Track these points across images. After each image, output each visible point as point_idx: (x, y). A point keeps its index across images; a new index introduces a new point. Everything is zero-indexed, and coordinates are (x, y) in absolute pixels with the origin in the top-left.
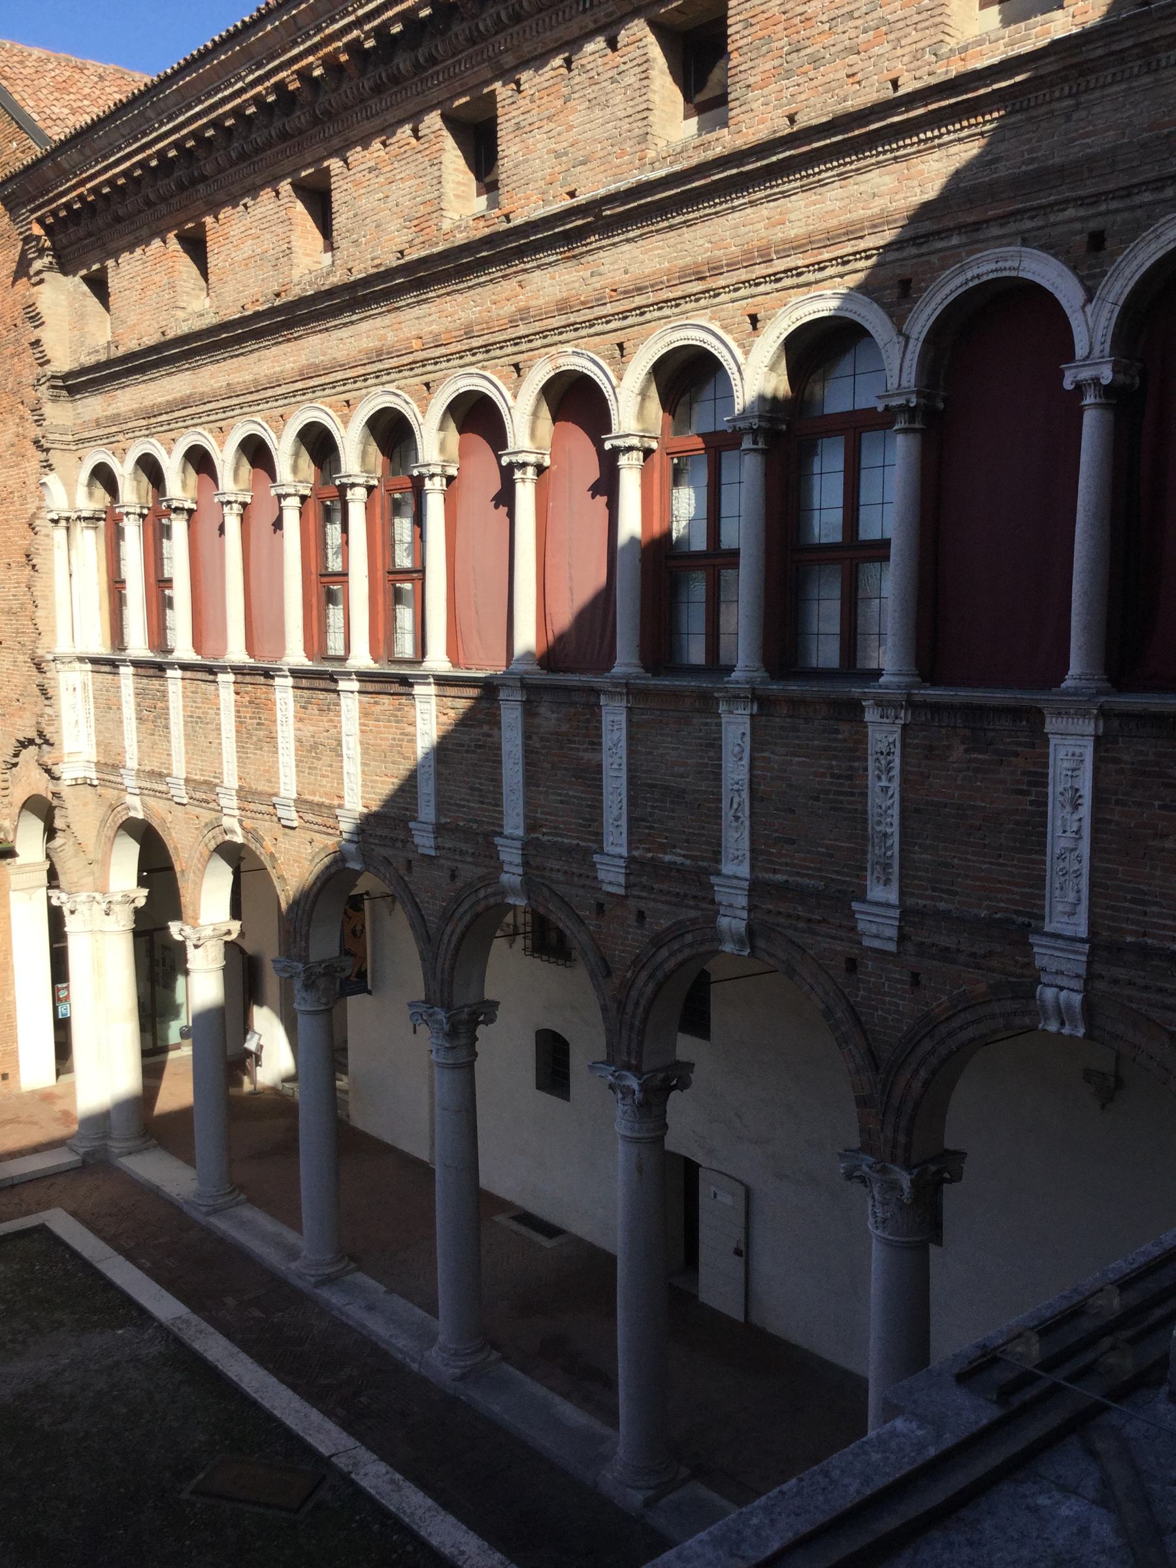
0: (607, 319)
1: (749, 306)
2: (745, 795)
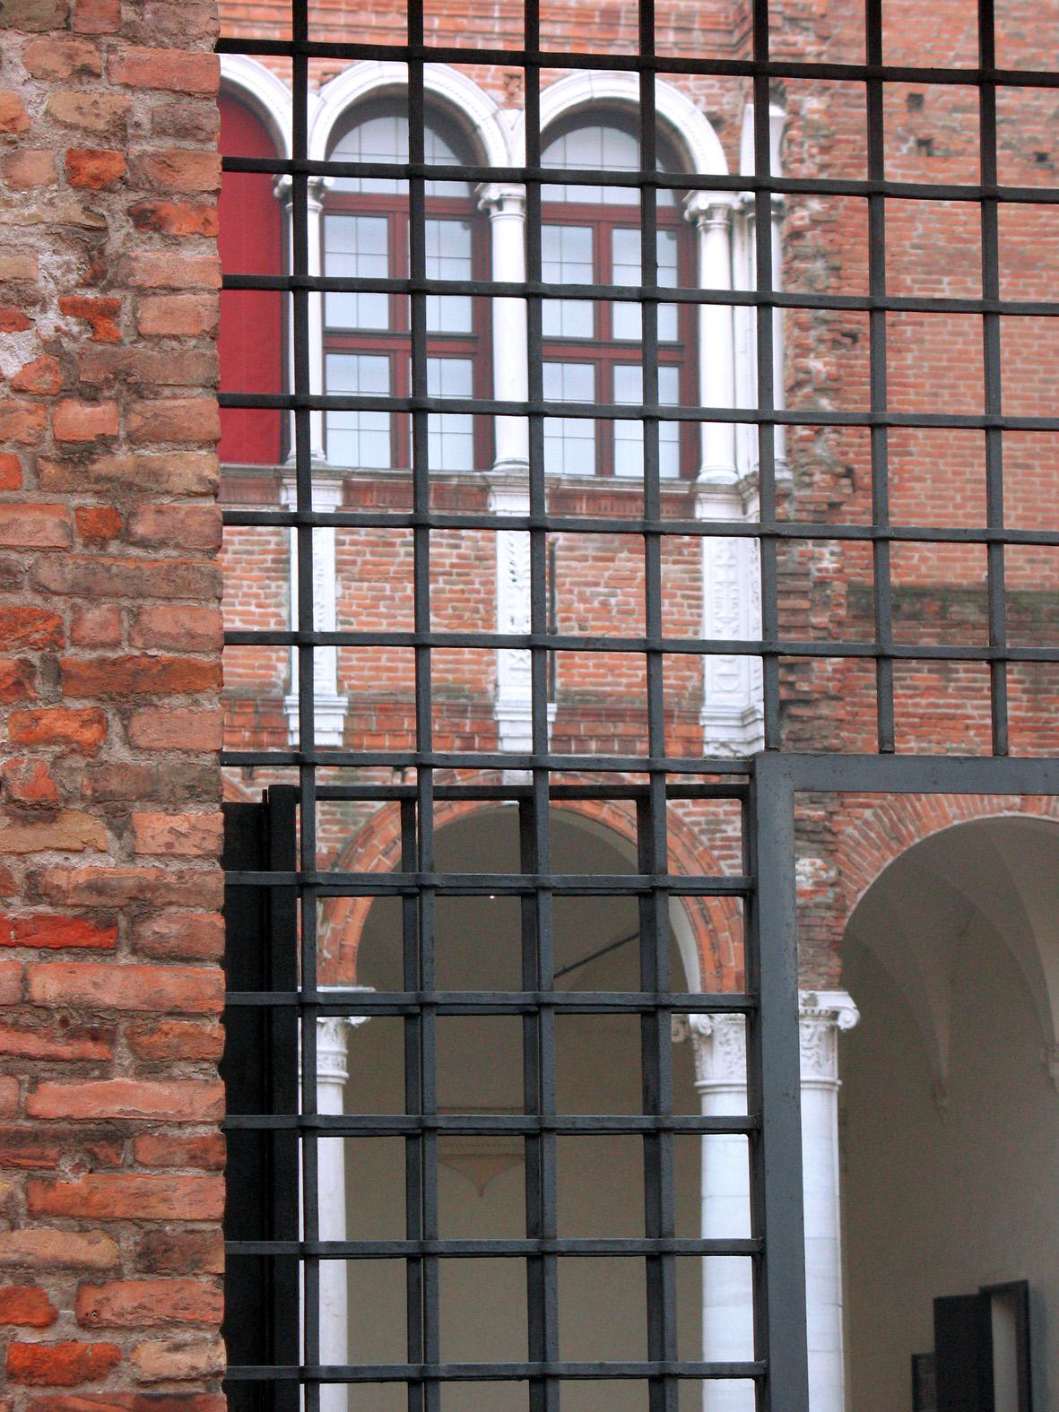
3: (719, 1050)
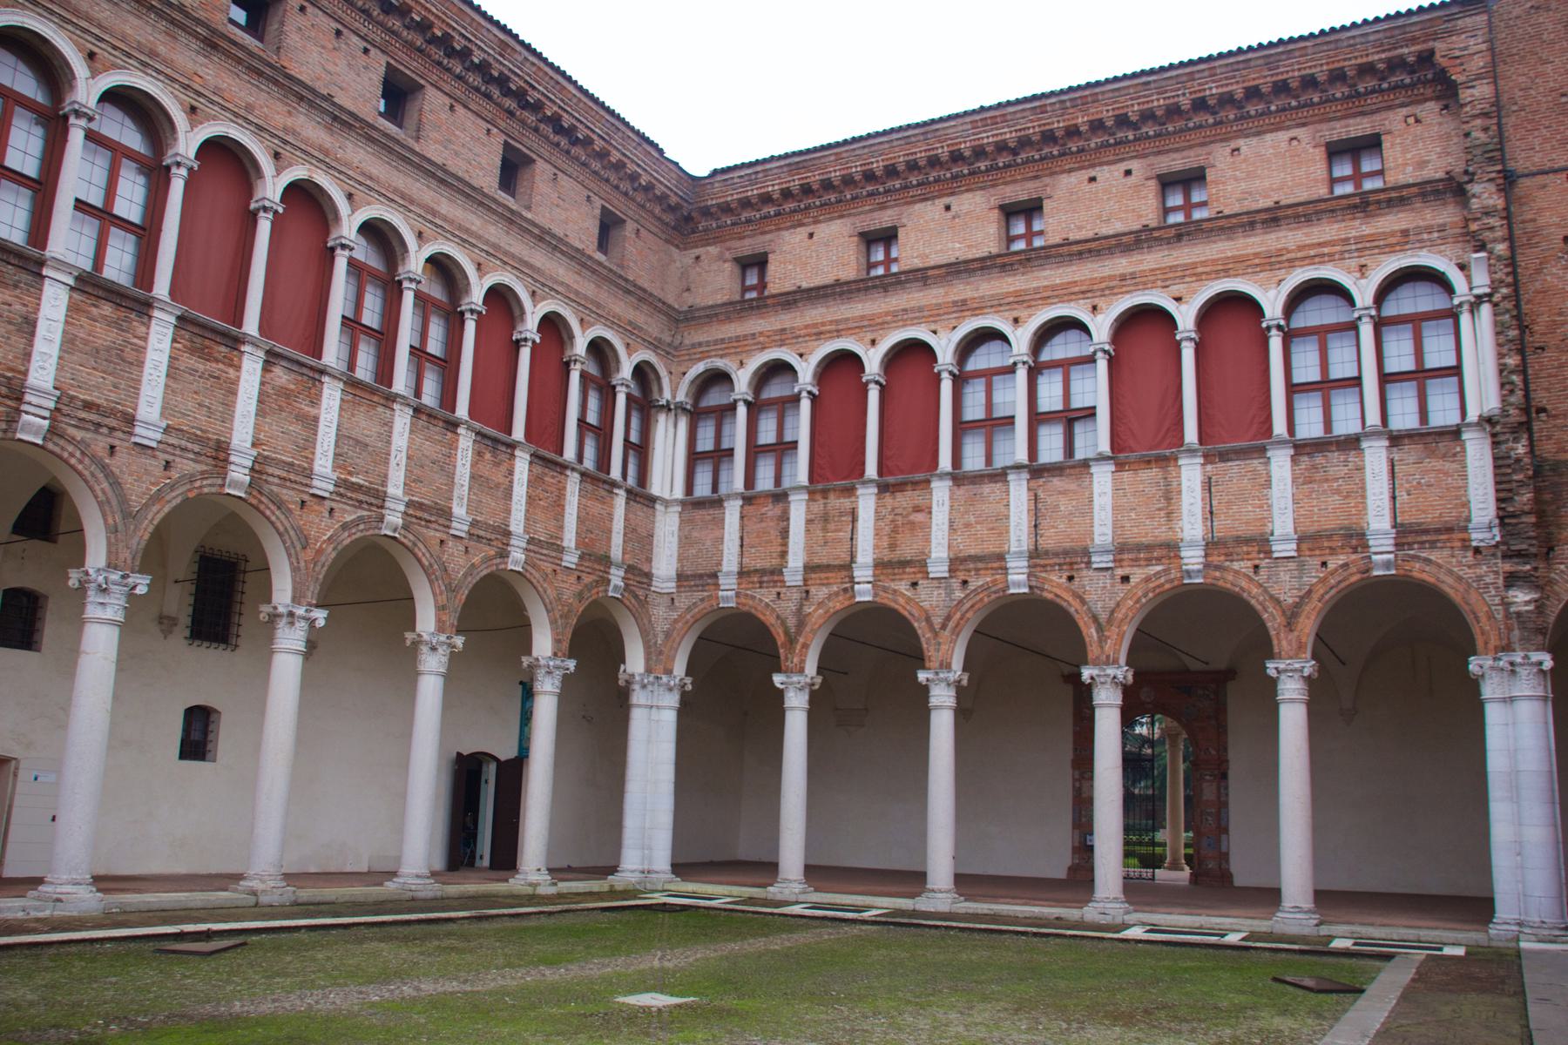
0: (350, 178)
1: (423, 229)
2: (404, 455)
3: (1488, 682)
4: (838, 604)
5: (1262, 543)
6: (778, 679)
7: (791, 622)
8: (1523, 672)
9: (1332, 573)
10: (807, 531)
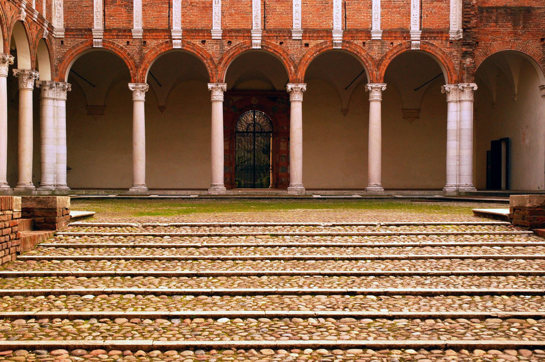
3: (451, 95)
4: (162, 50)
5: (368, 32)
6: (131, 86)
7: (137, 58)
8: (467, 91)
9: (395, 48)
10: (143, 10)
